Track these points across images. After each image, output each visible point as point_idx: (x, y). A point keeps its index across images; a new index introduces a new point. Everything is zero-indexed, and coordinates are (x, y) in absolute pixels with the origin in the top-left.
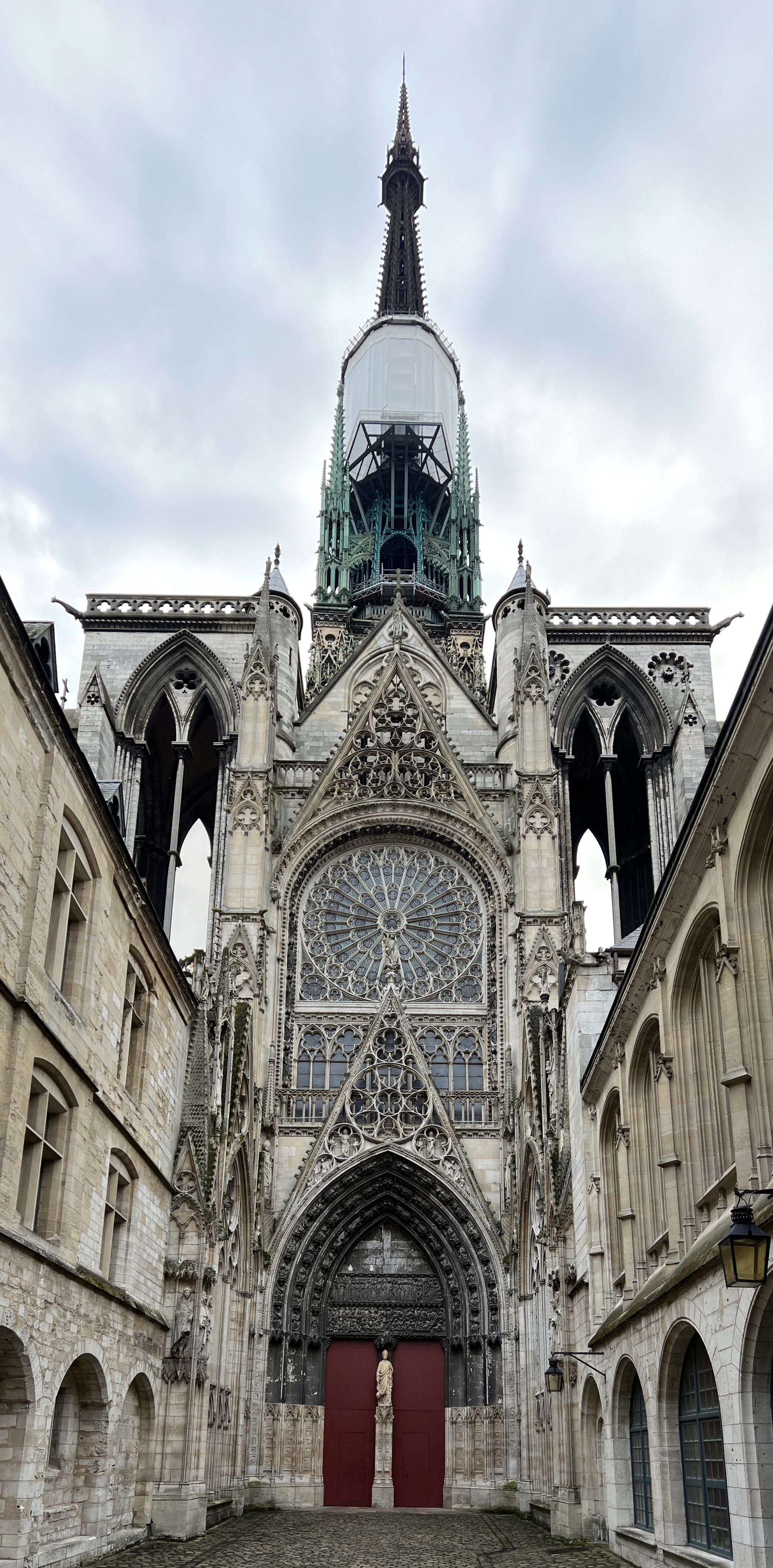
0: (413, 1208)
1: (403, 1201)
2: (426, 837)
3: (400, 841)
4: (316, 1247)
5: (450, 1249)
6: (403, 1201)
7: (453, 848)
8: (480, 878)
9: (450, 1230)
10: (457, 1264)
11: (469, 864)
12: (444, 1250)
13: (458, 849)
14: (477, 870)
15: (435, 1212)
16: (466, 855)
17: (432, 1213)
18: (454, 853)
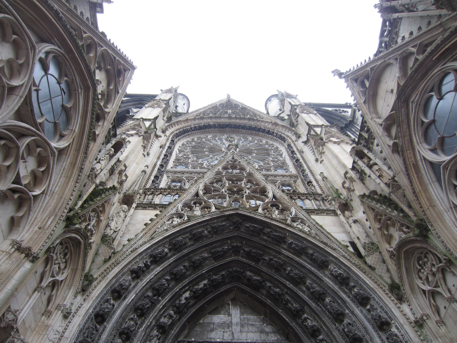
0: (264, 269)
1: (253, 264)
2: (247, 129)
3: (233, 132)
4: (154, 295)
5: (313, 305)
6: (253, 264)
7: (261, 132)
8: (278, 139)
9: (308, 282)
10: (325, 319)
11: (270, 136)
12: (306, 307)
13: (264, 131)
14: (275, 136)
15: (289, 268)
16: (268, 132)
17: (285, 270)
18: (261, 133)
